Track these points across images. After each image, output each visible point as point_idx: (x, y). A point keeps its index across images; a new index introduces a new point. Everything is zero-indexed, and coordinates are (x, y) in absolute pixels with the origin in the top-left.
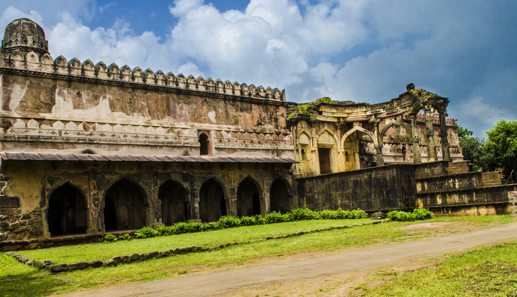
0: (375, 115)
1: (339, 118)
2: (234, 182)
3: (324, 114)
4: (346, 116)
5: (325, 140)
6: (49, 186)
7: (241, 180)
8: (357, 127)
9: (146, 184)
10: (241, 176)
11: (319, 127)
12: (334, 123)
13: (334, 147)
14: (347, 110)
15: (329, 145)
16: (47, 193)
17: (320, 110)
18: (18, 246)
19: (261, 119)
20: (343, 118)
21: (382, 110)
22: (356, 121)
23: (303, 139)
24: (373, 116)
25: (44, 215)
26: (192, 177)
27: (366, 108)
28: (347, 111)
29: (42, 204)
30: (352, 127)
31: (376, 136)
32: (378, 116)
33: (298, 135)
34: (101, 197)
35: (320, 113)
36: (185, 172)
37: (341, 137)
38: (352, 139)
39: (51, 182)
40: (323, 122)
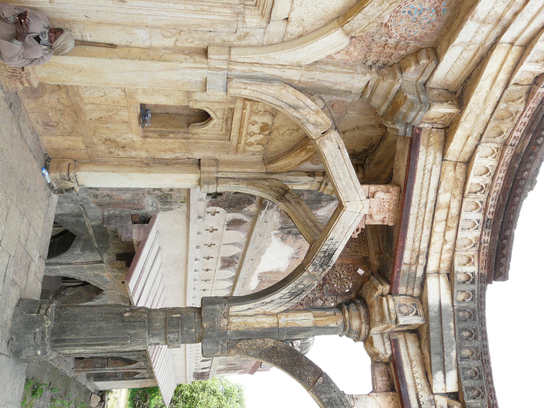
0: (415, 331)
1: (459, 94)
8: (361, 205)
13: (253, 20)
14: (491, 163)
20: (448, 129)
21: (452, 387)
24: (415, 321)
27: (470, 279)
28: (484, 160)
30: (365, 179)
31: (285, 321)
32: (408, 351)
37: (310, 91)
38: (281, 164)
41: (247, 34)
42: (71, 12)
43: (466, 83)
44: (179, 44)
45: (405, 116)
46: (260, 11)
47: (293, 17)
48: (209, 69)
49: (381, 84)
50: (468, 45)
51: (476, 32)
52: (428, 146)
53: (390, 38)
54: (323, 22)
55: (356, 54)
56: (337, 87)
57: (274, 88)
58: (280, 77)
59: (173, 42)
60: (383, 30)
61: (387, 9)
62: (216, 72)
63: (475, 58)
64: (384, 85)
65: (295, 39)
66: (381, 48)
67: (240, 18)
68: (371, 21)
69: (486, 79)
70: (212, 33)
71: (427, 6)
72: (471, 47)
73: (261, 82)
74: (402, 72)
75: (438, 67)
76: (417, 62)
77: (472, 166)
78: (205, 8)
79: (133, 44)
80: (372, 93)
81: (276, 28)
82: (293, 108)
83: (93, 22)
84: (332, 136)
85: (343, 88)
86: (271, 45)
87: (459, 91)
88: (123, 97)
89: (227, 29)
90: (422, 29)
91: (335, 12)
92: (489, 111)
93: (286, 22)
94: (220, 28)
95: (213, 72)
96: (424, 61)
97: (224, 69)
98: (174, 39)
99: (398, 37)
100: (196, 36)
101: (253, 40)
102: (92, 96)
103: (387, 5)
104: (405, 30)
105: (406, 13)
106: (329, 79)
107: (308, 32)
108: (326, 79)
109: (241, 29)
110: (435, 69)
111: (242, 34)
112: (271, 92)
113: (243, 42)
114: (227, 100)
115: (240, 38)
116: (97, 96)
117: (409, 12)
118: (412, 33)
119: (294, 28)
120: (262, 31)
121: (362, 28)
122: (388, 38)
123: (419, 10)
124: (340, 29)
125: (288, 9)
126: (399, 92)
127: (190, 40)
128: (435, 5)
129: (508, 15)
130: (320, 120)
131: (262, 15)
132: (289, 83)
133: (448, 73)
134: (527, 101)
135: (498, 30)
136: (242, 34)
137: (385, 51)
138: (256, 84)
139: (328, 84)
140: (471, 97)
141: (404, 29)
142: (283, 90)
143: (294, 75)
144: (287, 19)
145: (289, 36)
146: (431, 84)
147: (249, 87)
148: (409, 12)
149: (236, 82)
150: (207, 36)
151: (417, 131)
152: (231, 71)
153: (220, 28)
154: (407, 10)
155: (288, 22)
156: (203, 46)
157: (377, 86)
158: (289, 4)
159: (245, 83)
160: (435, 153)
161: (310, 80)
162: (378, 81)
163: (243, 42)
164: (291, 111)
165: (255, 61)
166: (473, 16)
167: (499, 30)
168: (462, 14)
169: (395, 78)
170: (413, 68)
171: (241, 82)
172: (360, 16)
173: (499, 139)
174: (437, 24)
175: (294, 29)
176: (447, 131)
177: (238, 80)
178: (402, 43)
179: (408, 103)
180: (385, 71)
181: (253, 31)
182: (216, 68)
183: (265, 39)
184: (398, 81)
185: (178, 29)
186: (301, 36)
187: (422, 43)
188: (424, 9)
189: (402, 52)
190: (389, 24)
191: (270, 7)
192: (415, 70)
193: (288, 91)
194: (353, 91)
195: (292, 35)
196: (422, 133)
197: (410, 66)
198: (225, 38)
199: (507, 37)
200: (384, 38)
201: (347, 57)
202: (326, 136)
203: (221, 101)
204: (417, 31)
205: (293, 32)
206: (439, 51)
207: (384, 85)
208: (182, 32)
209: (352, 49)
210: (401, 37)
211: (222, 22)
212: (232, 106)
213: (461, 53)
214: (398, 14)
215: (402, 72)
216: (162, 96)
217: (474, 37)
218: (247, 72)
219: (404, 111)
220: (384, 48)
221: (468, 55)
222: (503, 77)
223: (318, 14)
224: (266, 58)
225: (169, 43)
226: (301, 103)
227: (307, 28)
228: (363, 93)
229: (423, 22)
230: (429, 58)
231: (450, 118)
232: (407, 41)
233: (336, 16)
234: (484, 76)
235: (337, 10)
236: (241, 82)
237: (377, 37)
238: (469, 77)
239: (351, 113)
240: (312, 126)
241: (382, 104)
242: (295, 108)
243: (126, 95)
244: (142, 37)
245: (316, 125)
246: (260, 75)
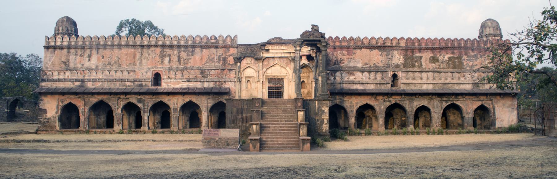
2: (177, 104)
5: (275, 71)
6: (61, 104)
7: (184, 103)
9: (113, 104)
10: (184, 100)
16: (60, 107)
17: (266, 48)
18: (45, 132)
19: (209, 59)
22: (304, 55)
23: (249, 72)
25: (57, 118)
26: (144, 100)
29: (57, 113)
33: (242, 70)
34: (87, 110)
36: (139, 97)
39: (62, 102)
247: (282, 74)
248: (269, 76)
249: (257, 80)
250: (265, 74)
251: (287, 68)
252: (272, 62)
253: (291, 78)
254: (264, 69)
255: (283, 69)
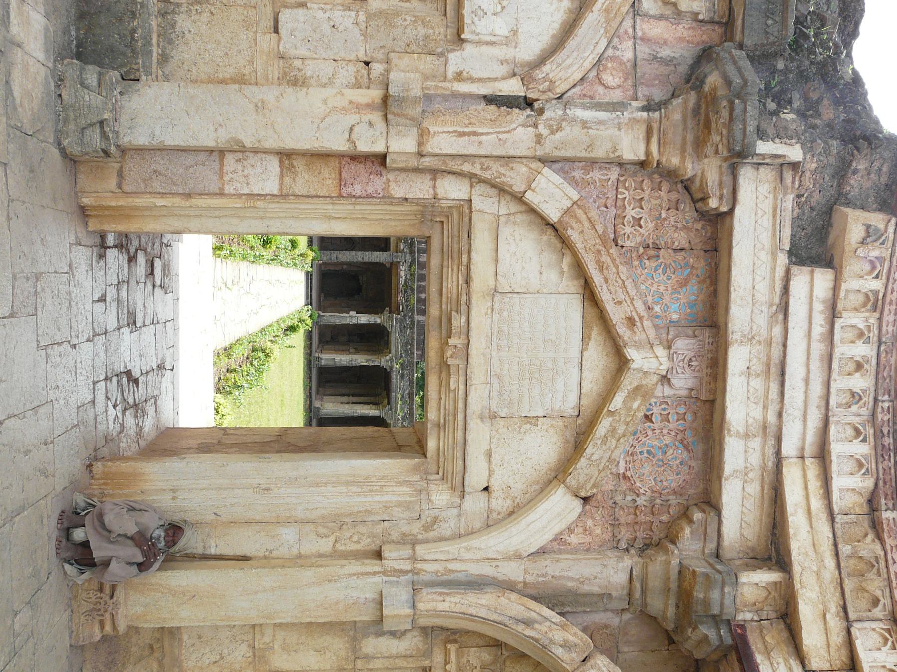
1: (774, 552)
3: (811, 286)
4: (812, 637)
11: (652, 249)
12: (704, 494)
13: (441, 496)
15: (457, 419)
17: (855, 224)
20: (787, 617)
35: (814, 245)
40: (710, 320)
41: (435, 520)
42: (198, 509)
43: (776, 534)
44: (340, 547)
45: (706, 603)
46: (449, 485)
47: (495, 485)
48: (385, 573)
49: (650, 568)
50: (746, 474)
51: (746, 452)
52: (768, 653)
53: (638, 495)
54: (537, 487)
55: (598, 531)
56: (586, 588)
57: (488, 596)
58: (494, 578)
59: (331, 544)
60: (624, 486)
61: (616, 448)
62: (395, 579)
63: (766, 491)
64: (656, 568)
65: (504, 519)
66: (632, 516)
67: (423, 496)
68: (601, 468)
69: (796, 511)
70: (386, 523)
71: (668, 440)
72: (751, 475)
73: (465, 589)
74: (673, 542)
75: (723, 519)
76: (690, 521)
77: (862, 667)
78: (375, 488)
79: (275, 553)
80: (644, 591)
81: (475, 504)
82: (524, 623)
83: (223, 522)
84: (599, 662)
85: (594, 588)
86: (472, 533)
87: (774, 554)
88: (250, 659)
89: (406, 514)
90: (677, 475)
91: (550, 470)
92: (830, 563)
93: (486, 493)
94: (397, 512)
95: (391, 579)
96: (697, 516)
97: (407, 572)
98: (332, 539)
99: (649, 493)
100: (363, 529)
101: (446, 528)
102: (199, 664)
103: (614, 442)
104: (655, 480)
105: (646, 455)
106: (570, 574)
107: (521, 505)
108: (565, 574)
109: (427, 512)
110: (720, 523)
111: (428, 519)
112: (483, 602)
113: (432, 534)
114: (418, 649)
115: (427, 528)
116: (208, 661)
117: (649, 452)
118: (665, 484)
119: (500, 501)
120: (455, 511)
121: (592, 481)
122: (635, 497)
123: (660, 448)
124: (562, 485)
125: (487, 473)
126: (682, 570)
127: (355, 538)
128: (679, 437)
129: (772, 418)
130: (571, 638)
131: (453, 488)
132: (508, 586)
133: (741, 526)
134: (879, 537)
135: (772, 442)
136: (428, 519)
137: (639, 518)
138: (458, 593)
139: (570, 584)
140: (790, 544)
141: (651, 478)
142: (502, 598)
143: (513, 571)
144: (486, 489)
145: (494, 516)
146: (726, 553)
147: (448, 599)
148: (649, 452)
149: (428, 594)
150: (379, 529)
151: (739, 631)
152: (417, 574)
153: (397, 512)
154: (645, 449)
155: (490, 494)
156: (374, 547)
157: (647, 579)
158: (486, 465)
159: (440, 594)
160: (786, 660)
161: (541, 579)
162: (645, 566)
163: (432, 534)
164: (520, 628)
165: (451, 557)
166: (729, 430)
167: (773, 442)
168: (717, 438)
169: (667, 551)
170: (687, 531)
171: (435, 593)
172: (582, 462)
173: (877, 612)
174: (693, 464)
175: (500, 503)
176: (788, 622)
177: (430, 590)
178: (658, 501)
179: (700, 580)
180: (649, 551)
181: (444, 514)
182: (395, 571)
183: (463, 524)
184: (673, 552)
185: (337, 522)
186: (511, 513)
187: (686, 497)
188: (667, 445)
189: (665, 518)
190: (629, 474)
191: (462, 474)
192: (692, 533)
193: (509, 599)
194: (614, 594)
195: (499, 514)
196: (749, 633)
197: (682, 529)
198: (405, 529)
199: (789, 448)
200: (629, 498)
201: (588, 539)
202: (588, 664)
203: (408, 652)
204: (672, 480)
205: (500, 508)
206: (713, 501)
207: (656, 568)
208: (344, 526)
209: (589, 522)
210: (653, 492)
211: (399, 504)
212: (426, 663)
213: (743, 488)
214: (636, 458)
215: (673, 542)
216: (312, 652)
217: (746, 460)
218: (442, 575)
219: (701, 596)
220: (636, 514)
221: (754, 489)
222: (817, 504)
223: (527, 475)
224: (468, 549)
225: (325, 545)
226: (533, 615)
227: (518, 500)
228: (630, 594)
229: (675, 463)
230: (704, 511)
231: (780, 595)
232: (663, 498)
233: (553, 475)
234: (790, 509)
235: (552, 465)
236: (435, 593)
237: (619, 498)
238: (774, 526)
239: (626, 649)
240: (561, 649)
241: (666, 605)
242: (528, 623)
243: (254, 656)
244: (288, 539)
245: (566, 645)
246: (461, 577)
247: (479, 435)
248: (460, 254)
249: (407, 76)
250: (486, 204)
251: (558, 510)
252: (650, 295)
253: (435, 558)
254: (552, 194)
255: (542, 447)
